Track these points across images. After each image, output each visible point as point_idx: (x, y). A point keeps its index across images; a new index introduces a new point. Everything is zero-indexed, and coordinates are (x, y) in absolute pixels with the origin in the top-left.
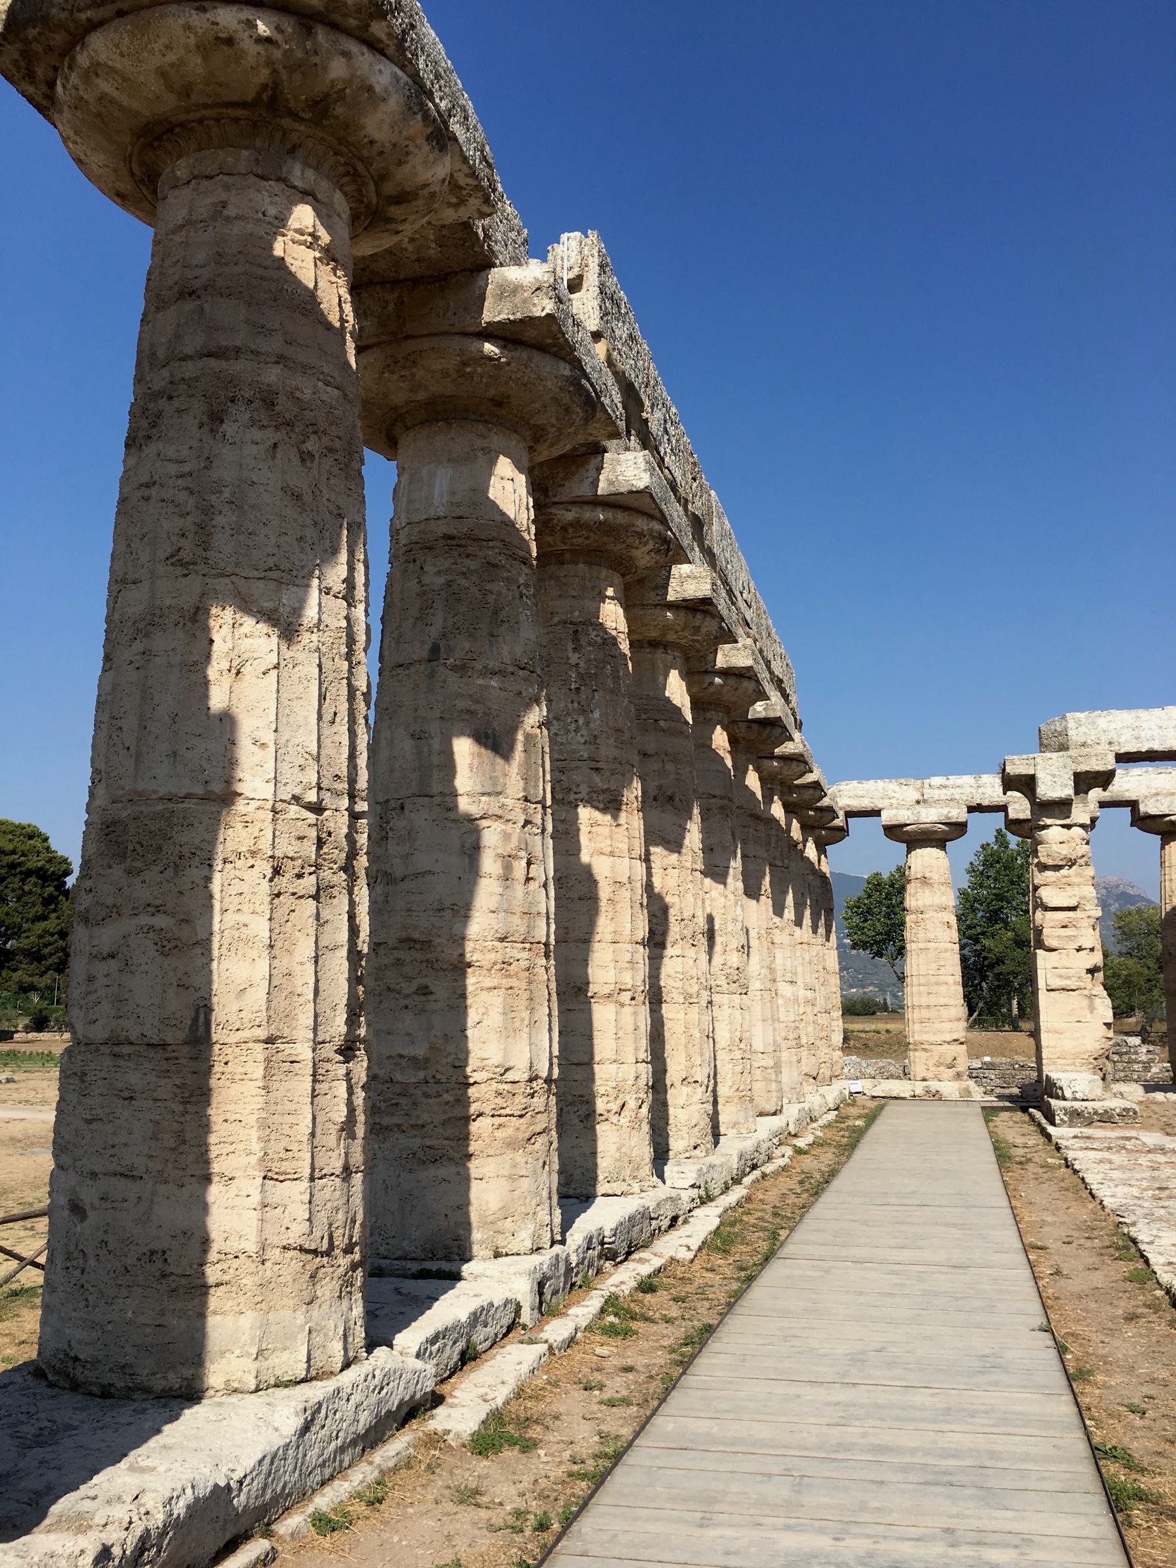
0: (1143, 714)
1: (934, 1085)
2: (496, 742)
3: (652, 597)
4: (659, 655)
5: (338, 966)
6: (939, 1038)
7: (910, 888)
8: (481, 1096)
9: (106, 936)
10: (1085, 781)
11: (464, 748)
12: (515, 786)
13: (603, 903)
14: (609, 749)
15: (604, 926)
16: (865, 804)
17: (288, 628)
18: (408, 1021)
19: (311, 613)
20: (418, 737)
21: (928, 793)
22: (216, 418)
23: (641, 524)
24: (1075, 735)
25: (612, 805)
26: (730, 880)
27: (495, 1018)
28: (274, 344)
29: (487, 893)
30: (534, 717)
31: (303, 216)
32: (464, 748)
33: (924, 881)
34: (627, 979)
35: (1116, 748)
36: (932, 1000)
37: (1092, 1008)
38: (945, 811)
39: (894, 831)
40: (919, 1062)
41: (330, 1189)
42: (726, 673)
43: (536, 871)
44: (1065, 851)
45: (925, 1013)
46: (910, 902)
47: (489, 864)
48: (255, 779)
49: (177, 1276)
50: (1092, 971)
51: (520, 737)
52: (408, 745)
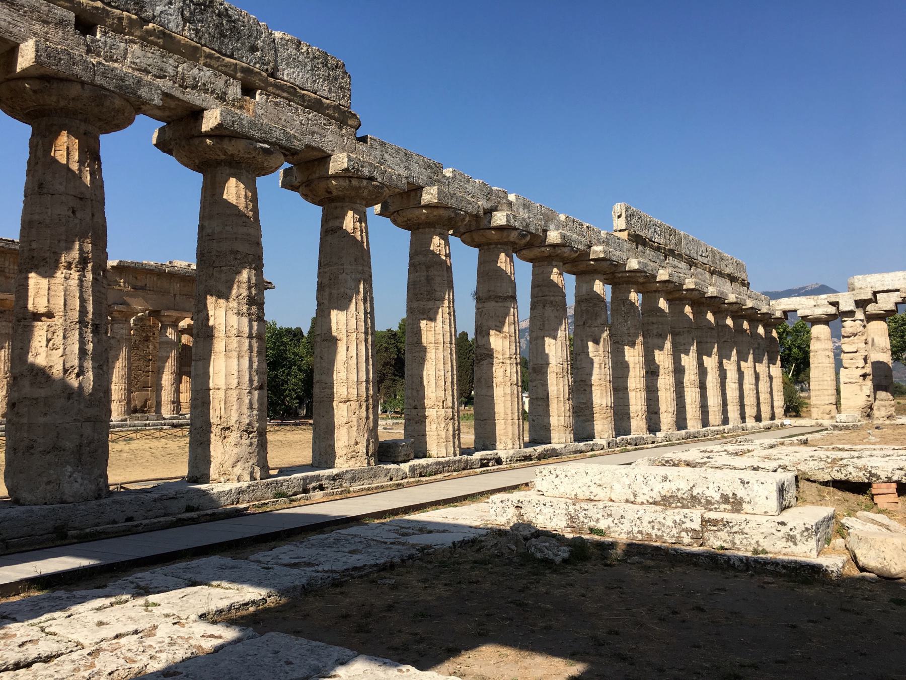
0: (886, 275)
1: (820, 421)
2: (596, 342)
3: (652, 280)
4: (657, 294)
5: (567, 387)
6: (823, 403)
7: (812, 342)
8: (596, 409)
9: (534, 384)
10: (861, 304)
11: (590, 344)
12: (601, 352)
13: (631, 369)
14: (632, 331)
15: (631, 373)
16: (792, 307)
17: (555, 338)
18: (582, 396)
19: (559, 335)
20: (582, 341)
21: (819, 302)
22: (544, 306)
23: (638, 275)
24: (857, 285)
25: (633, 344)
26: (691, 353)
27: (599, 395)
28: (551, 294)
29: (596, 371)
30: (605, 335)
31: (555, 270)
32: (590, 344)
33: (818, 338)
34: (638, 386)
35: (874, 289)
36: (820, 387)
37: (861, 390)
38: (825, 310)
39: (804, 318)
40: (815, 412)
41: (567, 418)
42: (687, 290)
43: (607, 366)
44: (851, 330)
45: (817, 393)
46: (812, 348)
47: (596, 365)
48: (553, 361)
49: (547, 428)
50: (864, 376)
51: (602, 340)
52: (580, 342)
